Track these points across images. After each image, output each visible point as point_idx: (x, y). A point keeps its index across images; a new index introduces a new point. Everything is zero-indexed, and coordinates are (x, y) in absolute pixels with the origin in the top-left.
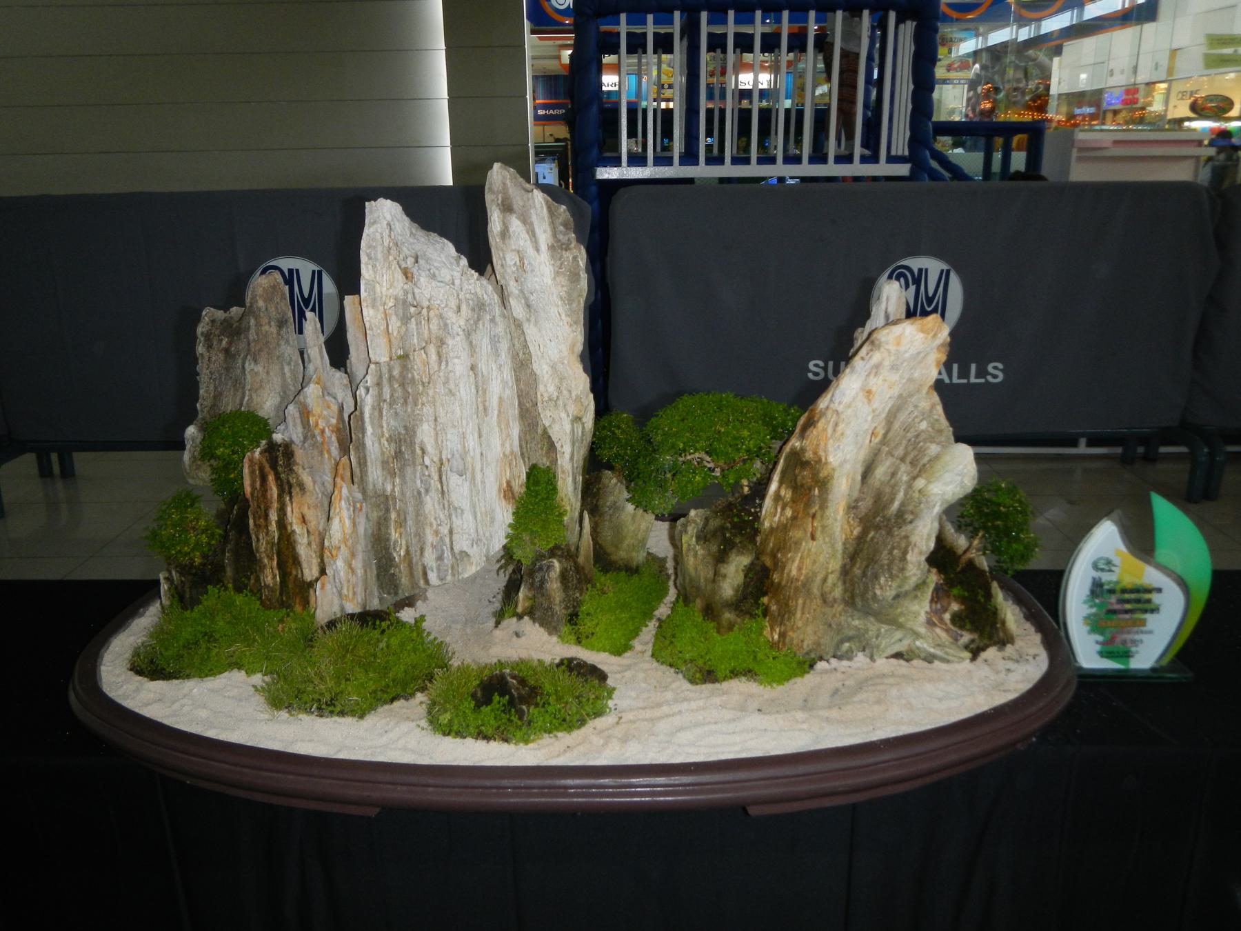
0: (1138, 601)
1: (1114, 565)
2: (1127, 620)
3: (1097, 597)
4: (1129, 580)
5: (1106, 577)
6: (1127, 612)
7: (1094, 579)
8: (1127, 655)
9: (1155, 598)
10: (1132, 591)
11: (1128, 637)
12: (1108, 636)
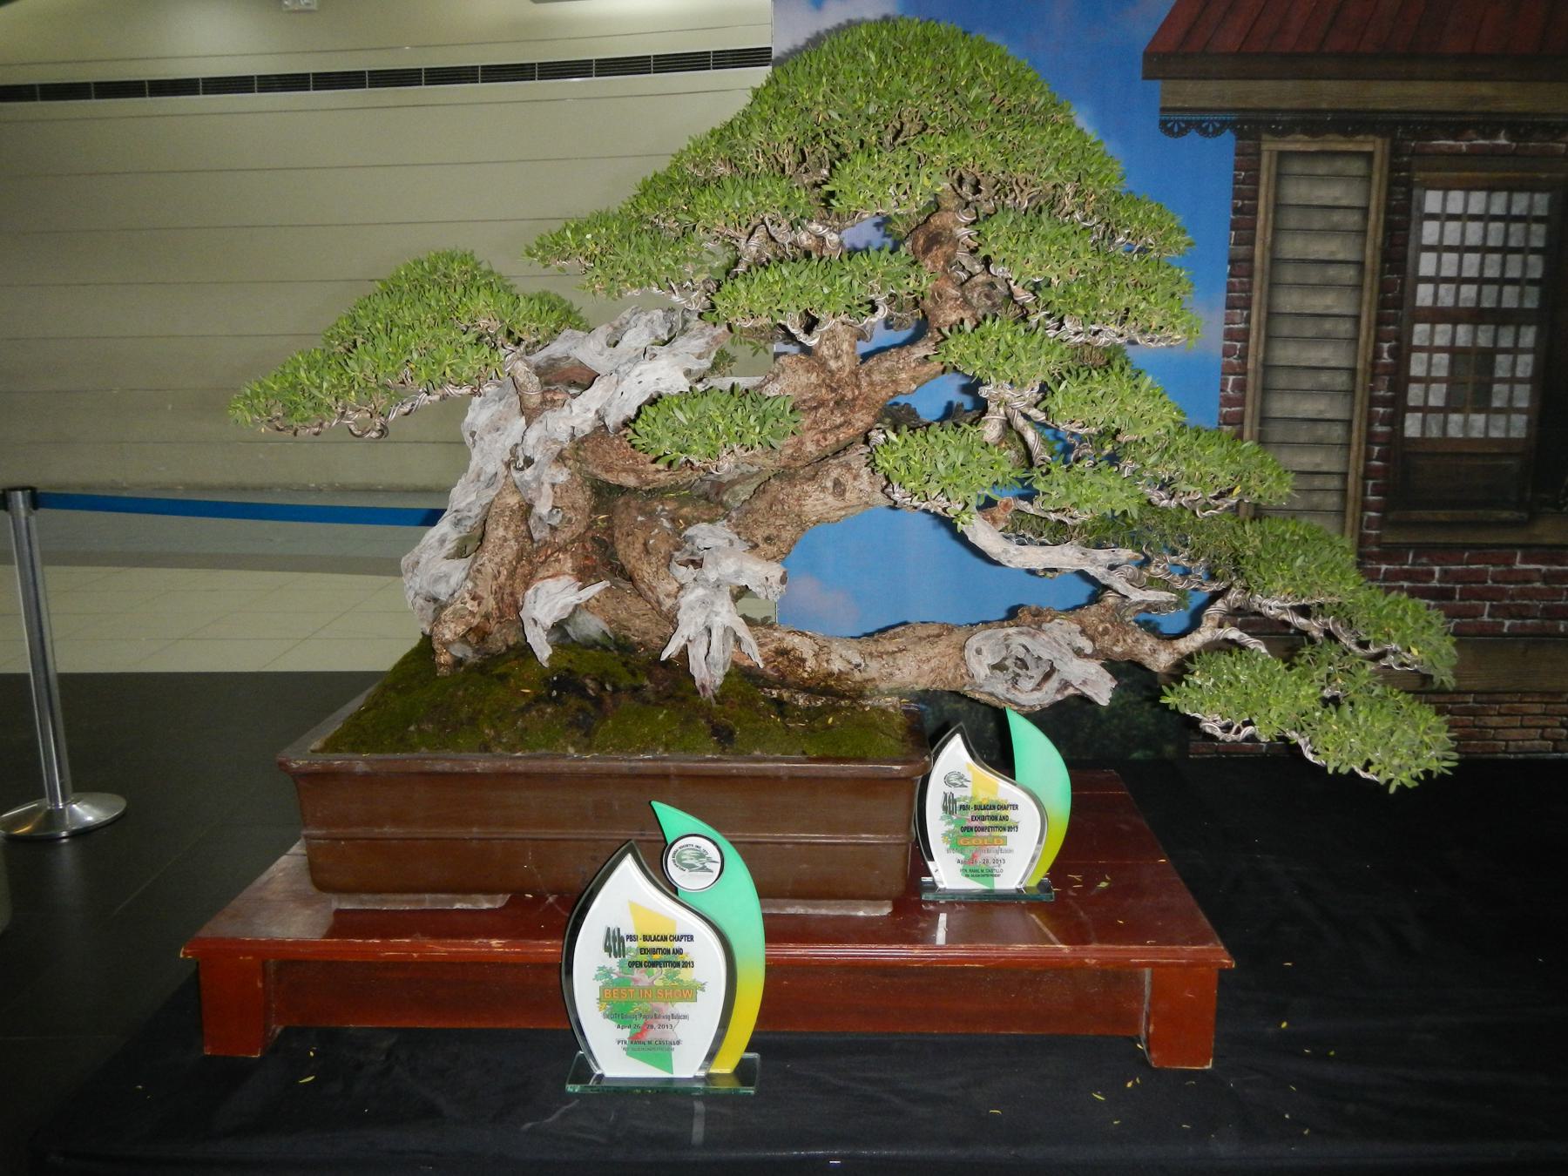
0: (994, 818)
4: (983, 797)
5: (958, 793)
6: (983, 829)
8: (990, 874)
9: (1010, 813)
11: (991, 856)
12: (969, 852)
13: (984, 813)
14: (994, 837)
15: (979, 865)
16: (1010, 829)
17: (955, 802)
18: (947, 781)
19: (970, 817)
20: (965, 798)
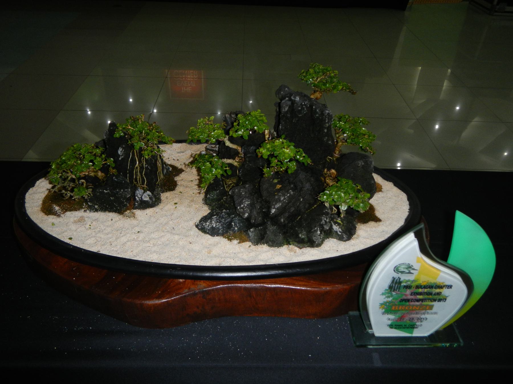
2: (417, 306)
4: (424, 279)
5: (404, 277)
8: (413, 327)
9: (445, 292)
10: (425, 287)
14: (424, 305)
15: (406, 321)
16: (440, 300)
20: (409, 281)
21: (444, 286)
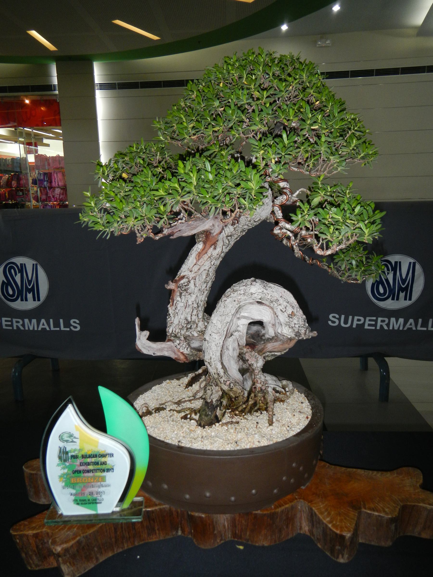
0: (97, 463)
1: (75, 438)
3: (65, 461)
4: (88, 449)
5: (69, 447)
6: (88, 471)
7: (60, 448)
8: (94, 502)
9: (108, 460)
10: (90, 456)
11: (94, 490)
12: (79, 489)
13: (89, 460)
14: (96, 476)
16: (108, 470)
17: (67, 453)
18: (61, 438)
19: (78, 463)
20: (75, 451)
21: (106, 455)
